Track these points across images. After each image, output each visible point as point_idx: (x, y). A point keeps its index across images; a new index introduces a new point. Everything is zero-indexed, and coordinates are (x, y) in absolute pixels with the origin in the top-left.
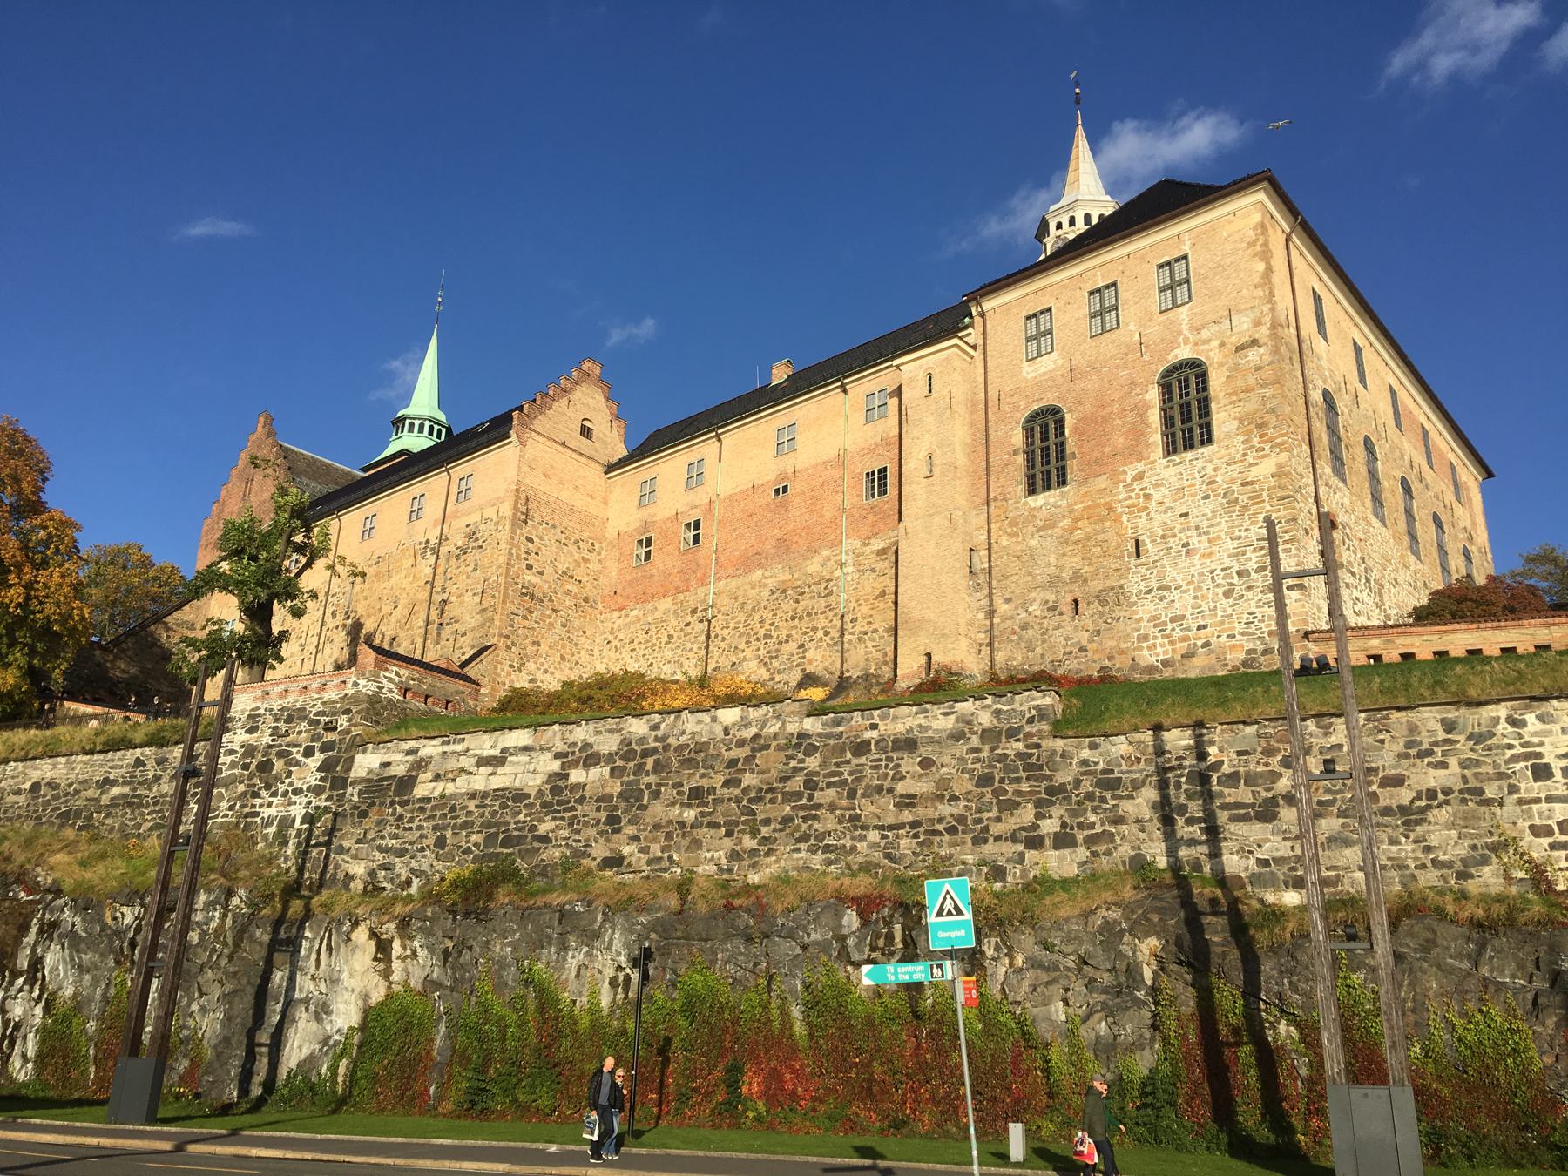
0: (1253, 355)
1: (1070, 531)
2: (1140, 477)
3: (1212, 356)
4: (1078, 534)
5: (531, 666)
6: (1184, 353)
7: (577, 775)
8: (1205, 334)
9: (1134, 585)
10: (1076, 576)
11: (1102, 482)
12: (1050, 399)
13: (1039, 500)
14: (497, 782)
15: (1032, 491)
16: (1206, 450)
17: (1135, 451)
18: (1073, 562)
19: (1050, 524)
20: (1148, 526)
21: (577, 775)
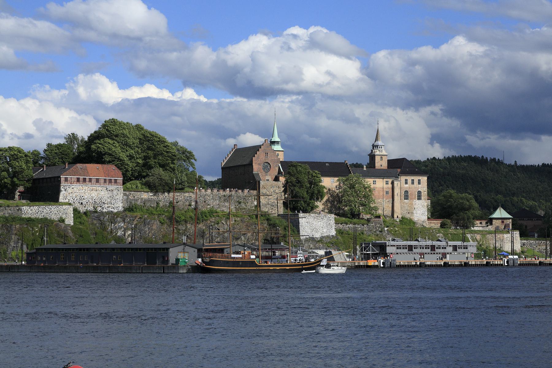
0: (425, 192)
1: (409, 205)
2: (415, 201)
3: (422, 191)
4: (409, 206)
6: (420, 190)
8: (422, 189)
9: (414, 212)
10: (409, 210)
11: (412, 201)
12: (407, 190)
13: (406, 201)
15: (405, 199)
16: (421, 201)
17: (415, 199)
18: (409, 208)
19: (407, 204)
20: (416, 207)
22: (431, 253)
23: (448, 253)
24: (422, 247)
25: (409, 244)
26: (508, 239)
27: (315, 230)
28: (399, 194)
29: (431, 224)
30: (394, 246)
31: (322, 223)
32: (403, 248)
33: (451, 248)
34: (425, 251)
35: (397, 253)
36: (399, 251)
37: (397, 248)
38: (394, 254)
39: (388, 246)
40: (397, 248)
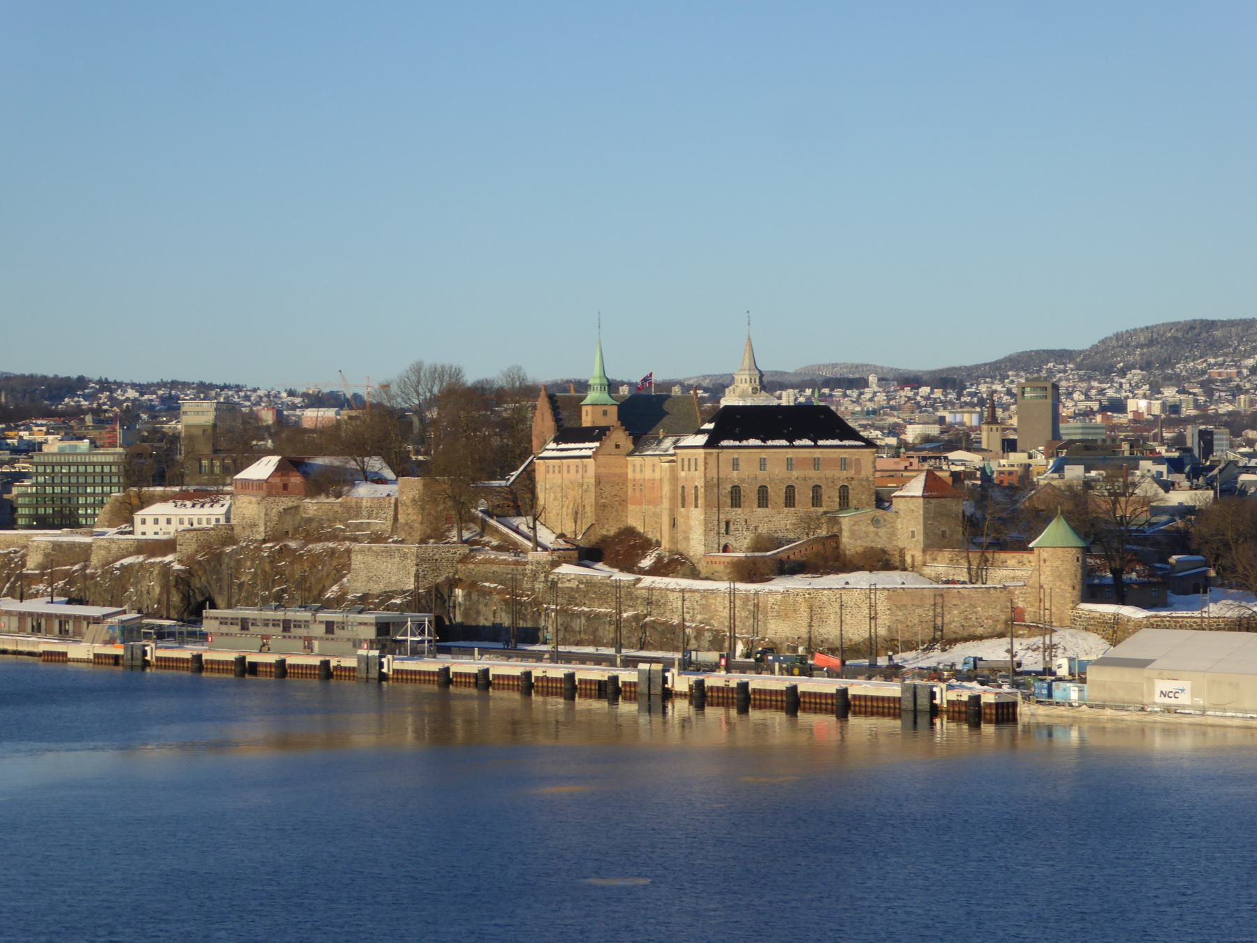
5: (606, 526)
6: (696, 484)
7: (580, 586)
13: (682, 510)
14: (570, 585)
21: (580, 586)
22: (327, 639)
23: (316, 638)
24: (266, 623)
25: (264, 617)
26: (776, 607)
27: (374, 578)
28: (668, 495)
29: (714, 565)
30: (217, 618)
31: (389, 565)
32: (232, 624)
33: (323, 627)
34: (271, 630)
35: (222, 634)
36: (224, 629)
37: (221, 623)
38: (216, 634)
39: (207, 618)
40: (221, 623)
